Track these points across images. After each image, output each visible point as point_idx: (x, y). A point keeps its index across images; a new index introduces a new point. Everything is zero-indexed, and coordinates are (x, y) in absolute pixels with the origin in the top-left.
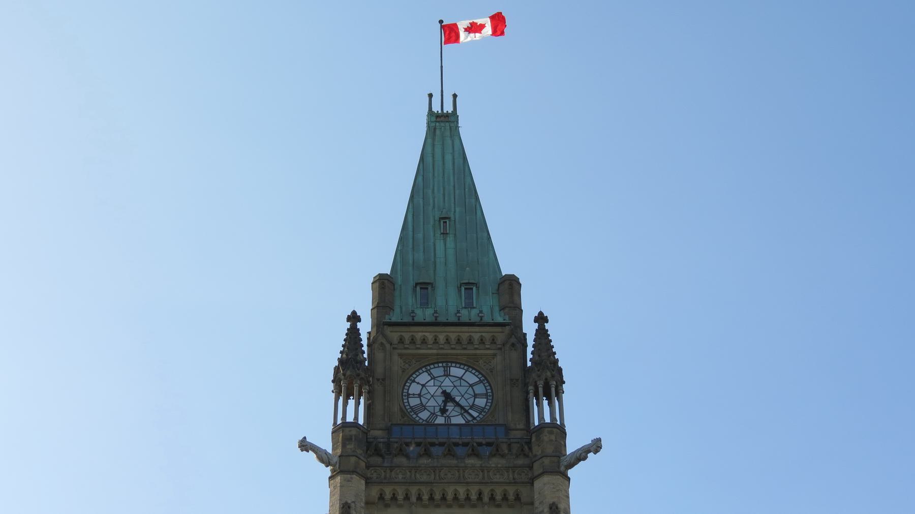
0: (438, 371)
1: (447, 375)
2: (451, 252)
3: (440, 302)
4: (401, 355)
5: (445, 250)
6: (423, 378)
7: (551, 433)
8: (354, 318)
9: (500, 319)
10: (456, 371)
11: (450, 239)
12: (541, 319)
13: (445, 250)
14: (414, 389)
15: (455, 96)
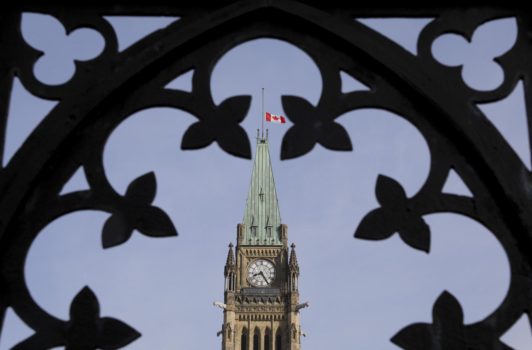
0: (259, 263)
1: (262, 265)
2: (264, 210)
3: (260, 235)
4: (247, 257)
5: (262, 208)
6: (254, 266)
7: (294, 295)
8: (230, 246)
9: (279, 244)
10: (265, 263)
11: (264, 203)
12: (293, 246)
13: (262, 208)
14: (251, 270)
15: (267, 130)
